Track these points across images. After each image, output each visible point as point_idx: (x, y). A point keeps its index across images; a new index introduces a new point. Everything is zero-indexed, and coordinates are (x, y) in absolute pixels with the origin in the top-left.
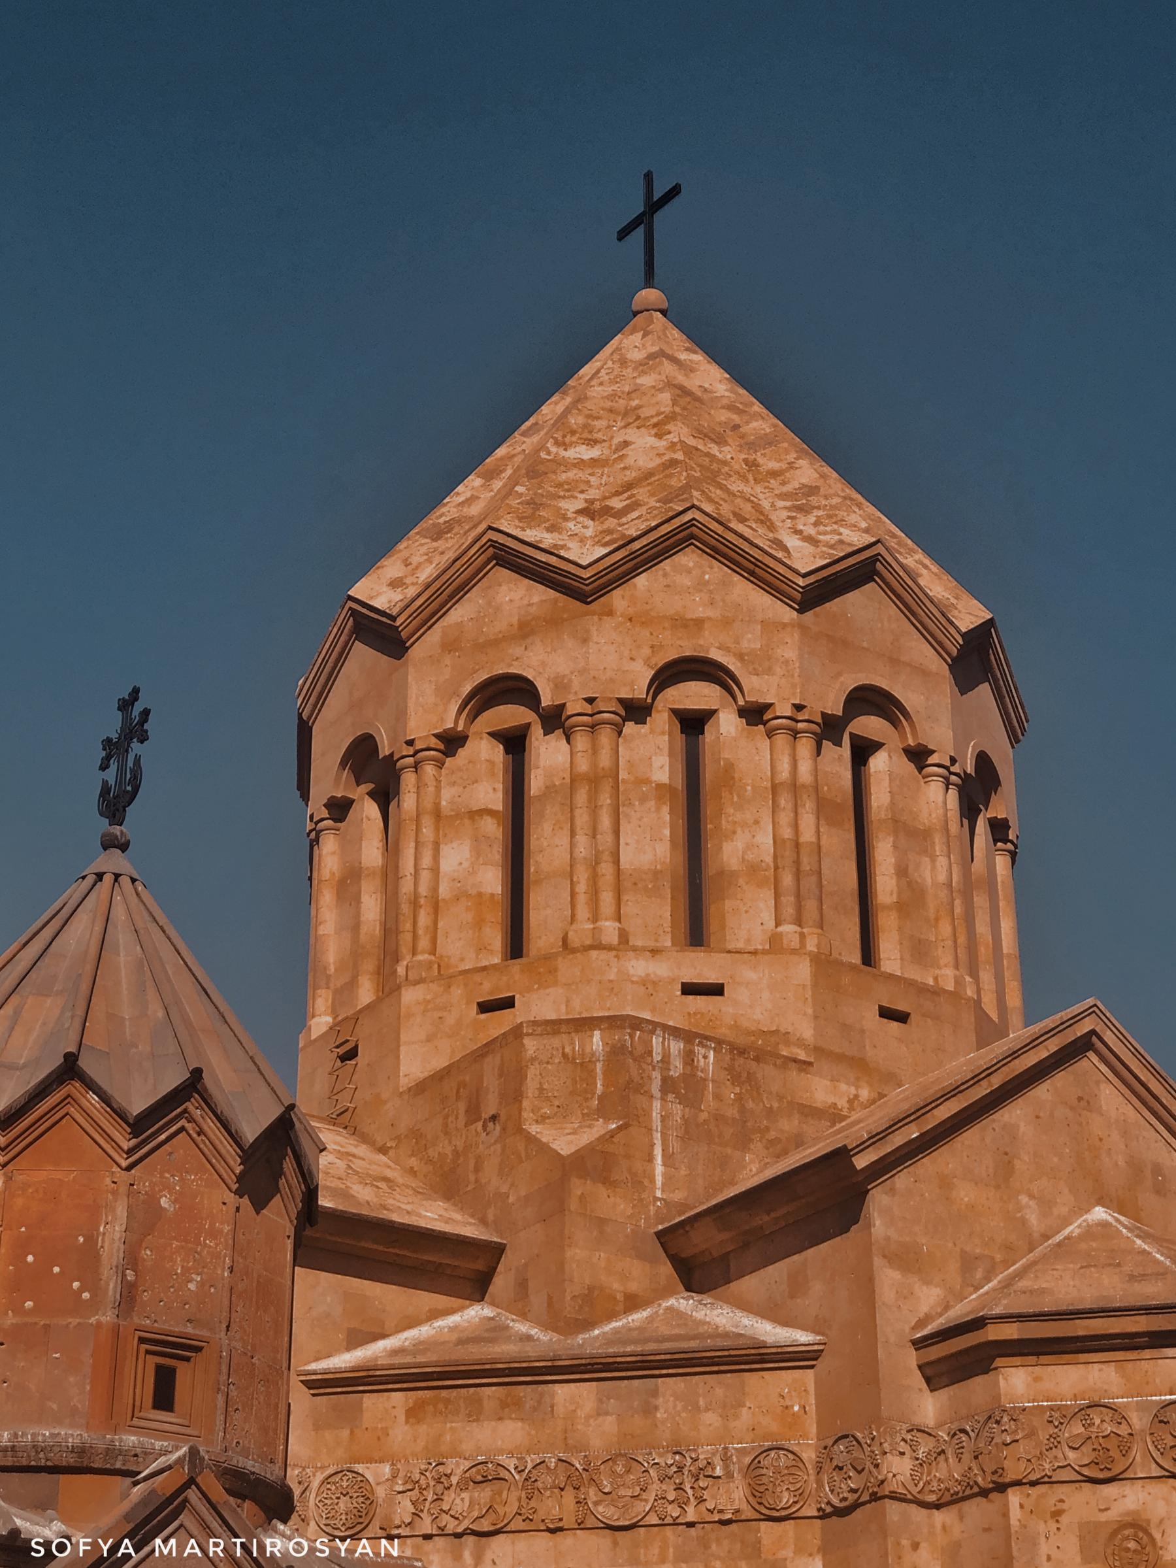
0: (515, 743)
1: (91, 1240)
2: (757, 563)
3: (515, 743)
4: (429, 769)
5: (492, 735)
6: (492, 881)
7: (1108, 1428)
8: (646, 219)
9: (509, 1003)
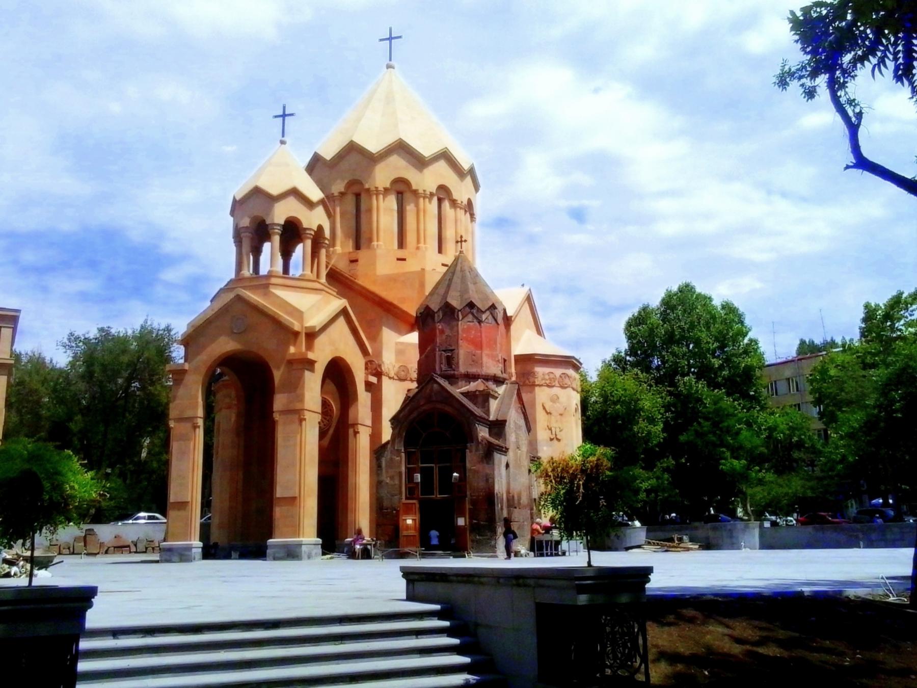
3: (400, 195)
4: (381, 197)
9: (404, 260)
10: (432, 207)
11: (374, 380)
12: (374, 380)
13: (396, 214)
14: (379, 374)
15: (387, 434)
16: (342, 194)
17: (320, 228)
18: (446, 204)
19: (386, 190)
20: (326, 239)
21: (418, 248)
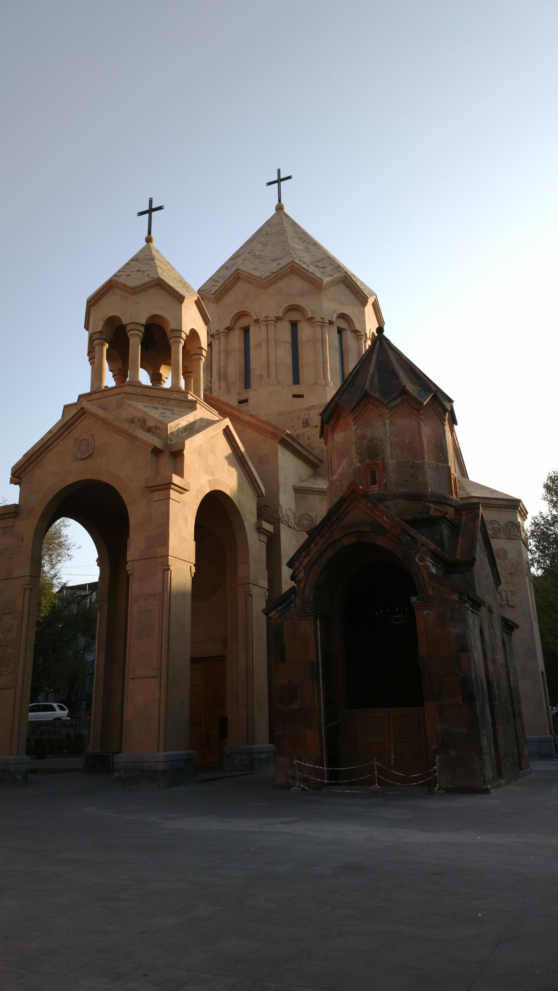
0: (294, 325)
1: (441, 443)
2: (358, 292)
3: (294, 325)
5: (289, 321)
6: (289, 361)
7: (496, 526)
8: (279, 181)
9: (302, 396)
10: (331, 337)
11: (269, 527)
12: (269, 527)
13: (289, 347)
14: (276, 521)
15: (287, 584)
16: (229, 329)
17: (194, 334)
18: (349, 337)
19: (278, 319)
20: (202, 348)
21: (316, 383)
